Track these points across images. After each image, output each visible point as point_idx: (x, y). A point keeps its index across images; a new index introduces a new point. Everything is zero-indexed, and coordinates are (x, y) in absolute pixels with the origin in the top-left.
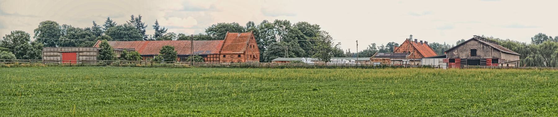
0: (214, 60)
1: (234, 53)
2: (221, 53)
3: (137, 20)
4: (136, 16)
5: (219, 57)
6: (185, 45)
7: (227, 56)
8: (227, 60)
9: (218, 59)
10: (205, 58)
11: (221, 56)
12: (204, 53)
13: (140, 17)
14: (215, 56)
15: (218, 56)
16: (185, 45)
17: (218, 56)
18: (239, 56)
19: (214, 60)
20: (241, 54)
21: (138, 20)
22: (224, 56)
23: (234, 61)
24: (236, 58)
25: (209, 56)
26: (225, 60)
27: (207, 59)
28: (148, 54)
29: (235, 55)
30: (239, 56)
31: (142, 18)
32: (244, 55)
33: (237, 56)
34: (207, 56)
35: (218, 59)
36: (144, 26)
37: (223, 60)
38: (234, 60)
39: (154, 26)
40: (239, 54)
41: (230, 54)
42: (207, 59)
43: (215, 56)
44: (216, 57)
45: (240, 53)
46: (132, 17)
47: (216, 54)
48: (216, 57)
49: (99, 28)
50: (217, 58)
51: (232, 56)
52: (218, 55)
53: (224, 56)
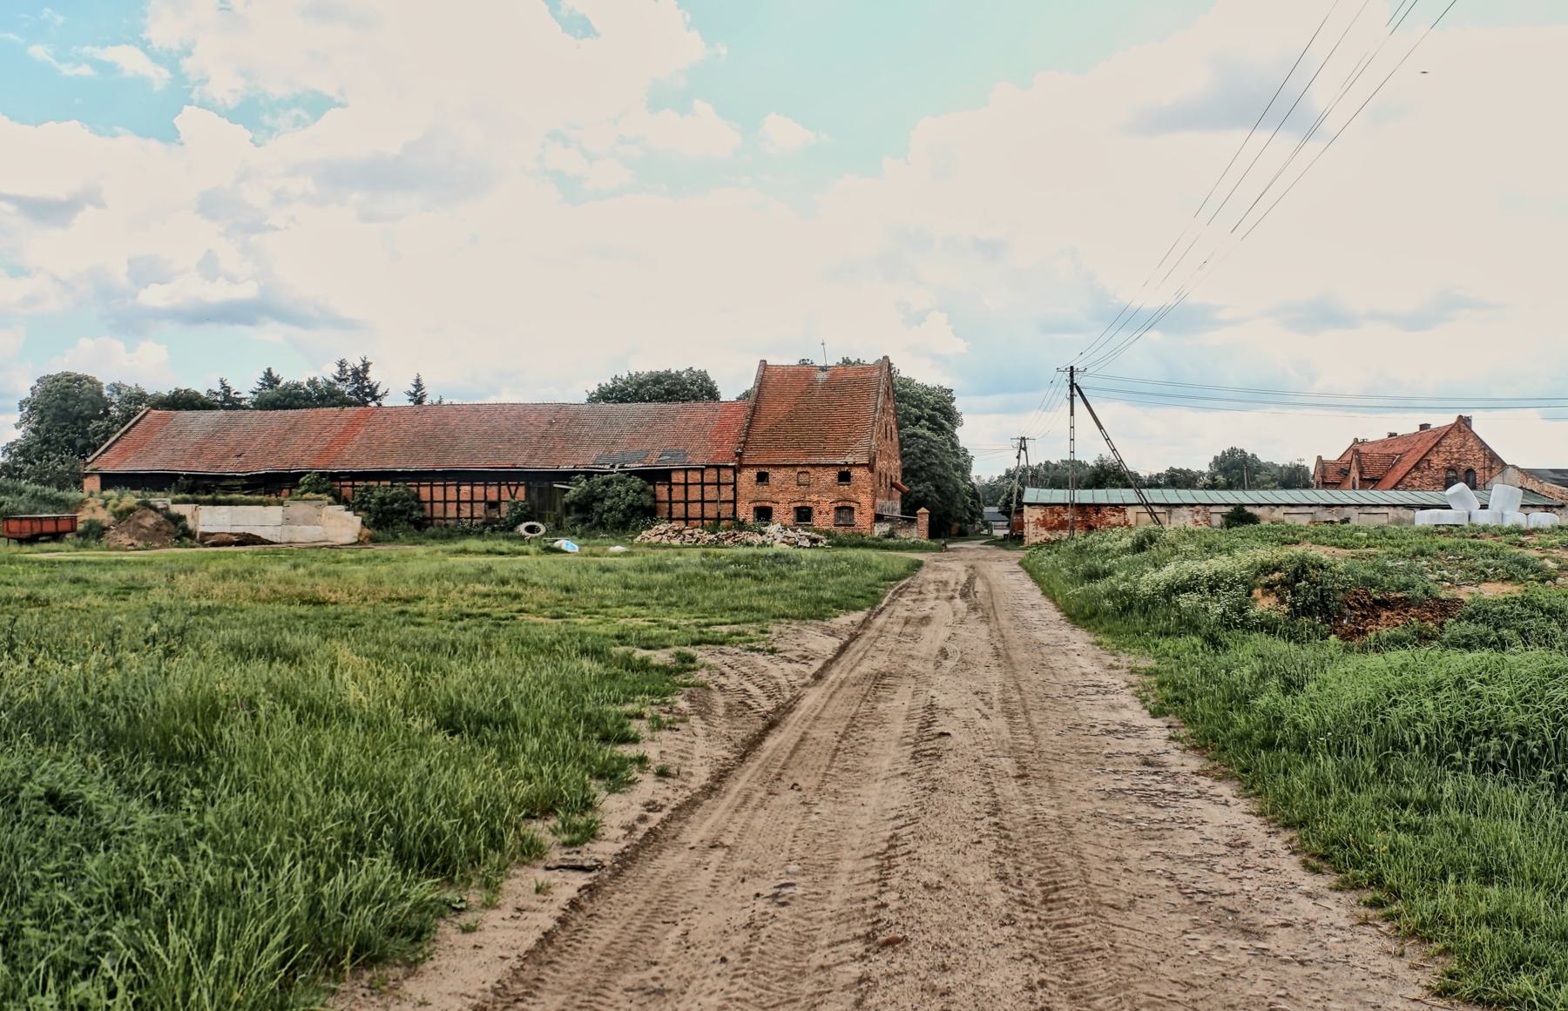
0: (707, 497)
1: (814, 460)
2: (745, 462)
3: (356, 373)
4: (355, 362)
5: (735, 483)
6: (551, 423)
7: (776, 476)
8: (774, 498)
9: (727, 493)
10: (658, 488)
11: (747, 477)
12: (653, 462)
13: (366, 366)
14: (711, 476)
15: (728, 475)
16: (551, 423)
17: (728, 475)
18: (845, 477)
19: (707, 497)
20: (854, 465)
21: (360, 375)
22: (762, 478)
23: (818, 502)
24: (830, 490)
25: (678, 477)
26: (766, 495)
27: (670, 490)
28: (369, 467)
29: (818, 473)
30: (845, 477)
31: (371, 368)
32: (872, 470)
33: (831, 476)
34: (669, 479)
35: (727, 493)
36: (379, 393)
37: (753, 496)
38: (815, 498)
39: (411, 394)
40: (846, 464)
41: (794, 466)
42: (670, 490)
43: (711, 476)
44: (719, 484)
45: (850, 460)
46: (342, 364)
47: (718, 468)
48: (719, 484)
49: (240, 400)
50: (723, 488)
51: (803, 478)
52: (730, 473)
53: (762, 478)
